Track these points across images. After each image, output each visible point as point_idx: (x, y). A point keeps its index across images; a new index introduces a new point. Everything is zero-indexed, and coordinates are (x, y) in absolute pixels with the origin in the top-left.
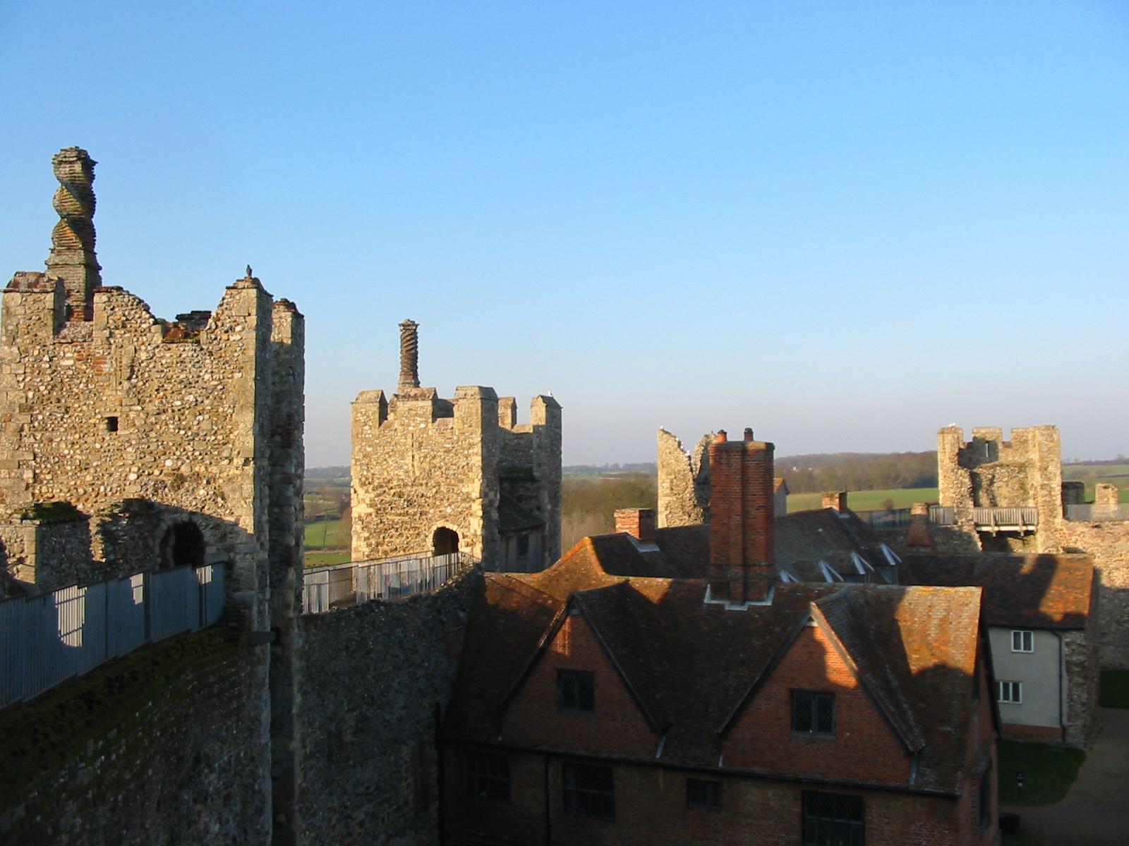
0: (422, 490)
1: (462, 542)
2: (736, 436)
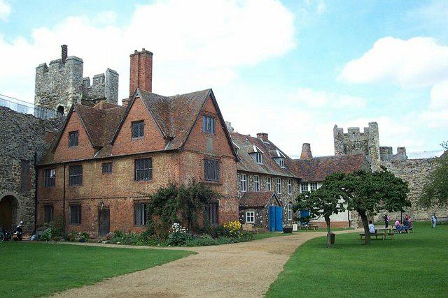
0: (54, 94)
2: (140, 50)
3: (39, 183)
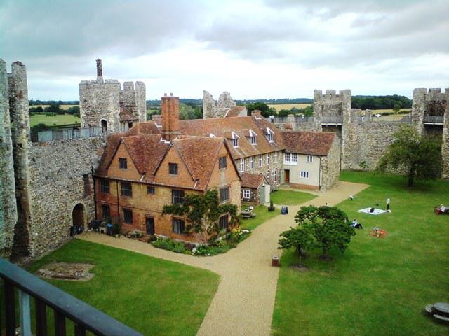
1: (108, 124)
2: (169, 95)
3: (97, 188)
